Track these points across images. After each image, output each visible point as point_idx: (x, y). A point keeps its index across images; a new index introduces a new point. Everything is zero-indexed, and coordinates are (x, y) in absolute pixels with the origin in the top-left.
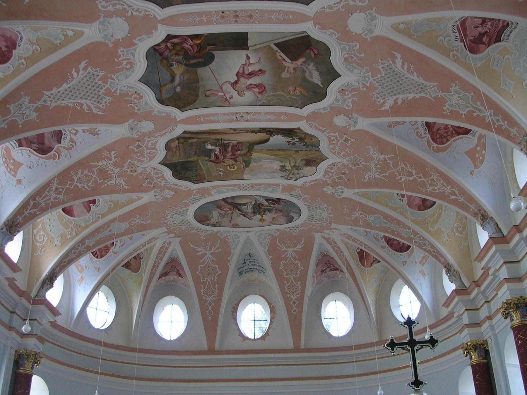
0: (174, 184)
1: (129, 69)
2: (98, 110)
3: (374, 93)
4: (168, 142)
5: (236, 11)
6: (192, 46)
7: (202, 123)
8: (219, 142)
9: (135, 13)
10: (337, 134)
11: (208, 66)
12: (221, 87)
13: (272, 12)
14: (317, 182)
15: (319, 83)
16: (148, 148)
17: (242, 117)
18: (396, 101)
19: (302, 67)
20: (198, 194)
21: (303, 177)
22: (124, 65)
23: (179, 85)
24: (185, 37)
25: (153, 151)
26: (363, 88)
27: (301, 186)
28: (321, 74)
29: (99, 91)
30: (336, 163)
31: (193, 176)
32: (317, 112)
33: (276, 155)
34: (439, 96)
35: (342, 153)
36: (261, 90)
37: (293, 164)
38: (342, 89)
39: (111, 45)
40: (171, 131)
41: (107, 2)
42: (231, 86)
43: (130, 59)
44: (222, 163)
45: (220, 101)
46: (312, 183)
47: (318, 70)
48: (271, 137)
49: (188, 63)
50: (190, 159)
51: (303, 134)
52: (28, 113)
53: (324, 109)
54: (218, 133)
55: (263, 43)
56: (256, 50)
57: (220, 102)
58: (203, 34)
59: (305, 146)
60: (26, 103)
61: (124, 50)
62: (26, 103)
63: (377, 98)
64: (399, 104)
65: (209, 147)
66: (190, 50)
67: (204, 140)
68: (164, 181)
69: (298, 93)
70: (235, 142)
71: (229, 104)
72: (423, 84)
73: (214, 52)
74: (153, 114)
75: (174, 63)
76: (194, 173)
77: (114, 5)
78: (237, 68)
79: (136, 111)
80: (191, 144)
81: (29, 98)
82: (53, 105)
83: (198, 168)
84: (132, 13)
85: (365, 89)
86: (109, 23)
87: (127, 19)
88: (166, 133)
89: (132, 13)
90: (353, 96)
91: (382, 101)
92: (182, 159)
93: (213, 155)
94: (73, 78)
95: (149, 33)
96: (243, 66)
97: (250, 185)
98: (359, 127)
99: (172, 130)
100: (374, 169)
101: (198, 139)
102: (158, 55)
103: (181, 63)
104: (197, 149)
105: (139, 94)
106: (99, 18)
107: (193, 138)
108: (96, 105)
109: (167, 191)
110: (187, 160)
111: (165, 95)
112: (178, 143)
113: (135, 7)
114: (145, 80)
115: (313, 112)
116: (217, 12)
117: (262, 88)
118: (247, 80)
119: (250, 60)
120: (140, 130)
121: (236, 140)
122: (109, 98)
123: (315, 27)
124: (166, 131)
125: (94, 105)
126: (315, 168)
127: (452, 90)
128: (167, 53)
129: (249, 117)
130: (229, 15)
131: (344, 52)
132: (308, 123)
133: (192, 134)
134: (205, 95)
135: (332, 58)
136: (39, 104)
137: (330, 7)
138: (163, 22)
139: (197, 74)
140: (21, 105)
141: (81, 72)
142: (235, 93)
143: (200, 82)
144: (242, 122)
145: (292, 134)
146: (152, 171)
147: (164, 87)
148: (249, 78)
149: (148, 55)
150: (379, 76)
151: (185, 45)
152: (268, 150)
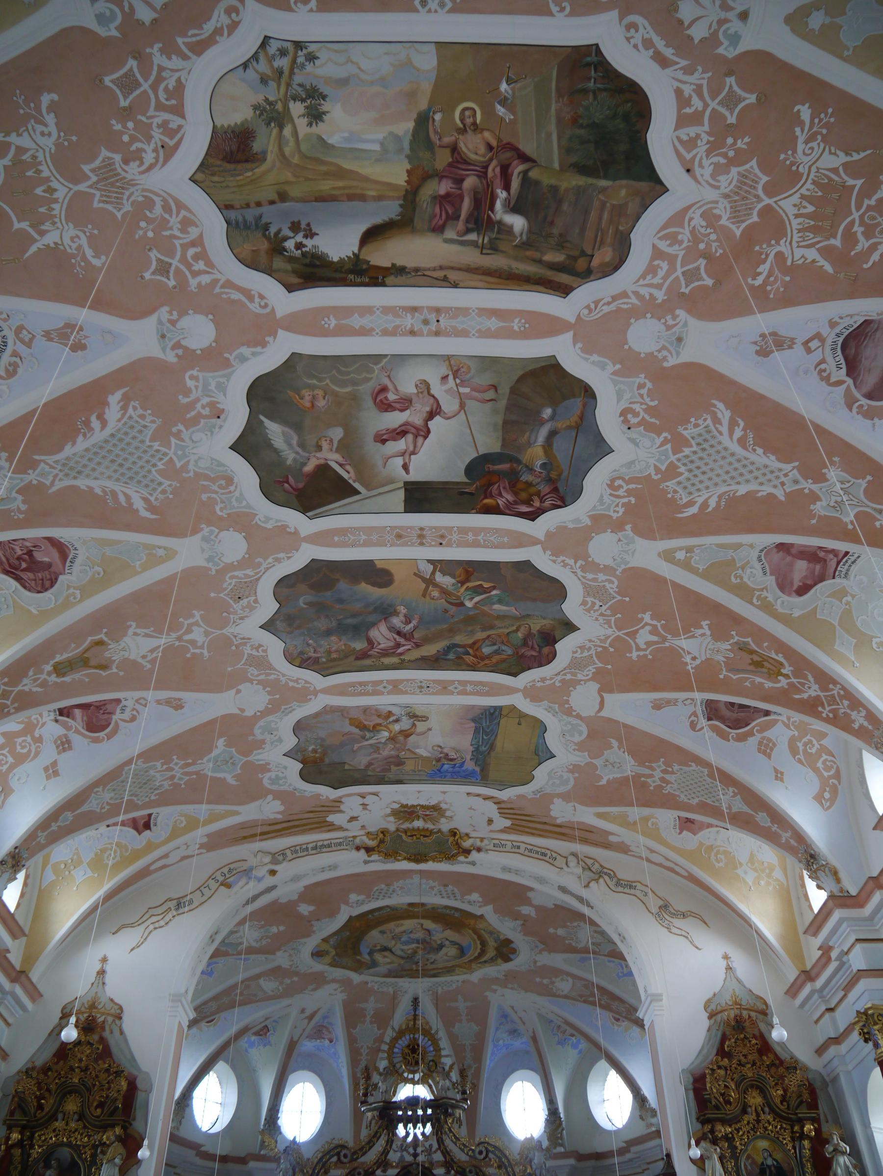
1: (619, 478)
2: (720, 415)
3: (155, 426)
4: (616, 268)
5: (421, 544)
6: (500, 495)
7: (520, 313)
8: (490, 240)
9: (571, 562)
10: (193, 283)
11: (481, 453)
12: (462, 406)
13: (367, 544)
14: (195, 35)
15: (267, 423)
16: (671, 259)
17: (426, 322)
18: (104, 423)
19: (307, 455)
21: (245, 66)
22: (625, 488)
23: (542, 422)
24: (508, 511)
25: (663, 245)
26: (179, 431)
28: (269, 444)
29: (695, 453)
30: (161, 159)
32: (255, 346)
33: (340, 173)
34: (30, 471)
35: (158, 210)
36: (381, 397)
37: (287, 131)
38: (219, 417)
39: (628, 527)
40: (596, 303)
41: (604, 586)
42: (443, 408)
43: (611, 495)
44: (494, 143)
45: (469, 372)
46: (209, 27)
47: (277, 451)
48: (356, 251)
49: (515, 465)
50: (581, 181)
51: (278, 271)
52: (838, 485)
53: (243, 359)
55: (380, 494)
56: (392, 482)
57: (469, 368)
58: (477, 513)
59: (264, 221)
60: (824, 503)
61: (611, 513)
62: (824, 503)
63: (142, 417)
64: (93, 418)
65: (518, 223)
66: (504, 488)
67: (528, 253)
68: (687, 90)
69: (306, 393)
70: (450, 234)
71: (452, 362)
72: (75, 478)
73: (466, 480)
74: (618, 366)
75: (538, 469)
77: (595, 580)
78: (428, 446)
79: (649, 385)
81: (812, 507)
82: (787, 467)
84: (575, 563)
85: (174, 430)
86: (614, 560)
87: (586, 556)
88: (609, 303)
89: (575, 563)
90: (192, 405)
91: (130, 411)
92: (604, 190)
93: (515, 183)
94: (720, 497)
95: (562, 529)
96: (417, 449)
98: (149, 324)
99: (593, 306)
100: (46, 173)
101: (540, 262)
102: (561, 490)
103: (527, 466)
104: (552, 223)
105: (626, 421)
106: (624, 571)
107: (553, 267)
108: (717, 429)
109: (698, 32)
111: (576, 404)
112: (593, 256)
113: (567, 570)
114: (602, 449)
115: (264, 344)
116: (449, 545)
117: (381, 401)
118: (410, 420)
119: (402, 463)
120: (663, 328)
121: (447, 241)
122: (685, 433)
123: (295, 528)
124: (607, 309)
125: (720, 428)
126: (218, 124)
127: (20, 498)
128: (544, 489)
129: (408, 321)
130: (433, 540)
131: (237, 494)
132: (268, 310)
134: (496, 390)
135: (256, 480)
136: (807, 485)
137: (278, 560)
138: (534, 541)
139: (504, 440)
140: (834, 507)
141: (700, 500)
142: (437, 390)
143: (500, 422)
144: (428, 307)
145: (306, 265)
146: (701, 159)
147: (573, 424)
148: (406, 424)
149: (577, 493)
150: (160, 466)
151: (510, 498)
152: (362, 198)
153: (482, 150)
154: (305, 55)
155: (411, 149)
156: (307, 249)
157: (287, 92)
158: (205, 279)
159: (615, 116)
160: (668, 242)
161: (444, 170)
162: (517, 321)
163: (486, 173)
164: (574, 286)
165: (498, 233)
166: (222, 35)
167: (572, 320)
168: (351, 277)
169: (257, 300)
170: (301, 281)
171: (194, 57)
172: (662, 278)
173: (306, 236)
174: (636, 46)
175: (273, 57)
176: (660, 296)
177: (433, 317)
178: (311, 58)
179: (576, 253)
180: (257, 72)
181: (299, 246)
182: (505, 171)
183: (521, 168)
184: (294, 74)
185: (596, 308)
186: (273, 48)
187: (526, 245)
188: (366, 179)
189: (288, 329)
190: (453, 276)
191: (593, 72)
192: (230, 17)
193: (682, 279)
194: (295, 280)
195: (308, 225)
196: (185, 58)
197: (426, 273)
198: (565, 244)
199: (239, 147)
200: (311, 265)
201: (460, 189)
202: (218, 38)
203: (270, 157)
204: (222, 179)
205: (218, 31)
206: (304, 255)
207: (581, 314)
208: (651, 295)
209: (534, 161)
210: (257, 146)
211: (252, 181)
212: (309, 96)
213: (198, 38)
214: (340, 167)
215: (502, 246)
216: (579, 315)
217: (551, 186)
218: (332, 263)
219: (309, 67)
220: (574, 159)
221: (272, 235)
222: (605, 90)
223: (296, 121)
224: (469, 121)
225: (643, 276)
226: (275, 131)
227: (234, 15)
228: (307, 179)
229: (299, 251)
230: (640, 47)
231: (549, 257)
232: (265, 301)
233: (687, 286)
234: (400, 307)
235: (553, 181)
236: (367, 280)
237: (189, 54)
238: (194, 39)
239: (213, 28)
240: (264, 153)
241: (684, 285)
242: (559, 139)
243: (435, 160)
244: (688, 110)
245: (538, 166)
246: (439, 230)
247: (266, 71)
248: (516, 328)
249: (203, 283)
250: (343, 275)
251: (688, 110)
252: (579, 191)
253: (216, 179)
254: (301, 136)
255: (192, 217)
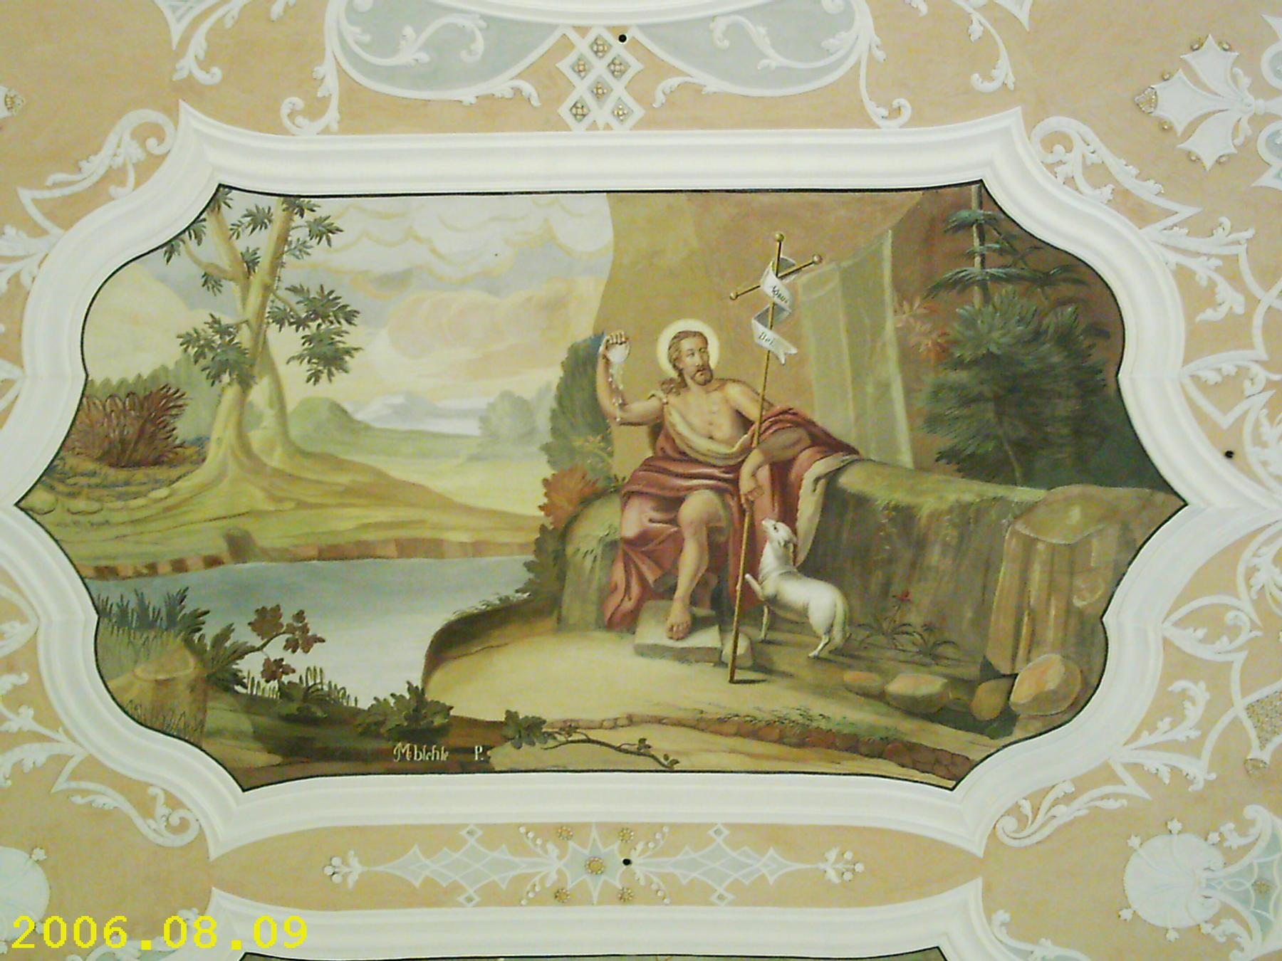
0: (1140, 213)
4: (1077, 706)
8: (752, 645)
16: (1215, 675)
20: (976, 30)
21: (170, 247)
25: (1190, 641)
27: (173, 113)
31: (976, 294)
37: (260, 393)
40: (1037, 798)
44: (753, 412)
46: (95, 167)
48: (417, 683)
50: (970, 491)
51: (218, 733)
54: (751, 729)
59: (189, 607)
67: (850, 676)
68: (1203, 270)
70: (652, 632)
76: (970, 323)
80: (930, 655)
83: (929, 379)
88: (1068, 798)
92: (1028, 510)
93: (808, 505)
97: (564, 111)
99: (1027, 808)
101: (881, 696)
104: (904, 598)
110: (993, 490)
120: (1217, 859)
133: (912, 748)
144: (601, 826)
145: (288, 719)
146: (1257, 424)
152: (434, 548)
153: (725, 427)
154: (309, 224)
155: (555, 431)
156: (294, 678)
157: (263, 306)
158: (34, 755)
159: (1037, 335)
160: (1201, 633)
161: (634, 475)
162: (832, 855)
163: (735, 482)
164: (975, 757)
165: (771, 627)
166: (122, 183)
167: (979, 851)
168: (403, 747)
169: (161, 810)
170: (277, 759)
171: (55, 230)
172: (1198, 726)
173: (292, 646)
174: (1070, 181)
175: (236, 230)
176: (1199, 770)
177: (615, 852)
178: (323, 231)
179: (972, 671)
180: (197, 262)
181: (274, 670)
182: (782, 475)
183: (821, 466)
184: (283, 264)
185: (1036, 811)
186: (238, 206)
187: (843, 655)
188: (445, 504)
189: (235, 888)
190: (661, 741)
191: (976, 242)
192: (143, 143)
193: (1248, 724)
194: (260, 758)
195: (300, 616)
196: (36, 231)
197: (593, 735)
198: (941, 650)
199: (142, 431)
200: (303, 719)
201: (674, 521)
202: (113, 189)
203: (214, 454)
204: (96, 506)
205: (114, 176)
206: (284, 692)
207: (999, 832)
208: (1174, 770)
209: (850, 450)
210: (184, 428)
211: (168, 509)
212: (316, 314)
213: (67, 191)
214: (379, 473)
215: (782, 660)
216: (993, 835)
217: (896, 508)
218: (357, 712)
219: (318, 250)
220: (944, 441)
221: (208, 641)
222: (1009, 279)
223: (283, 369)
224: (691, 362)
225: (1148, 724)
226: (231, 393)
227: (152, 143)
228: (301, 505)
229: (274, 684)
230: (1080, 181)
231: (905, 684)
232: (182, 813)
233: (1263, 742)
234: (530, 827)
235: (901, 497)
236: (444, 757)
237: (46, 224)
238: (57, 193)
239: (102, 171)
240: (201, 442)
241: (1255, 743)
242: (909, 392)
243: (611, 454)
244: (1209, 315)
245: (861, 460)
246: (624, 623)
247: (218, 262)
248: (832, 875)
249: (28, 765)
250: (385, 745)
251: (1209, 315)
252: (967, 518)
253: (80, 504)
254: (291, 406)
255: (15, 597)
